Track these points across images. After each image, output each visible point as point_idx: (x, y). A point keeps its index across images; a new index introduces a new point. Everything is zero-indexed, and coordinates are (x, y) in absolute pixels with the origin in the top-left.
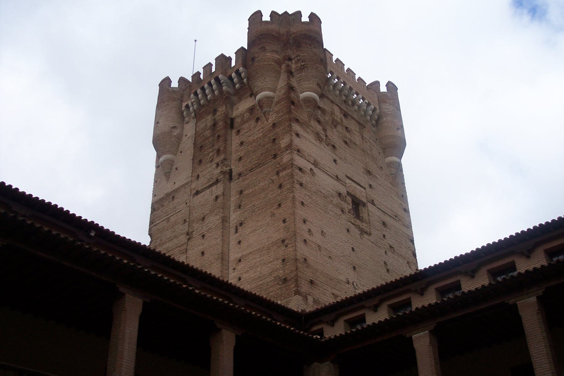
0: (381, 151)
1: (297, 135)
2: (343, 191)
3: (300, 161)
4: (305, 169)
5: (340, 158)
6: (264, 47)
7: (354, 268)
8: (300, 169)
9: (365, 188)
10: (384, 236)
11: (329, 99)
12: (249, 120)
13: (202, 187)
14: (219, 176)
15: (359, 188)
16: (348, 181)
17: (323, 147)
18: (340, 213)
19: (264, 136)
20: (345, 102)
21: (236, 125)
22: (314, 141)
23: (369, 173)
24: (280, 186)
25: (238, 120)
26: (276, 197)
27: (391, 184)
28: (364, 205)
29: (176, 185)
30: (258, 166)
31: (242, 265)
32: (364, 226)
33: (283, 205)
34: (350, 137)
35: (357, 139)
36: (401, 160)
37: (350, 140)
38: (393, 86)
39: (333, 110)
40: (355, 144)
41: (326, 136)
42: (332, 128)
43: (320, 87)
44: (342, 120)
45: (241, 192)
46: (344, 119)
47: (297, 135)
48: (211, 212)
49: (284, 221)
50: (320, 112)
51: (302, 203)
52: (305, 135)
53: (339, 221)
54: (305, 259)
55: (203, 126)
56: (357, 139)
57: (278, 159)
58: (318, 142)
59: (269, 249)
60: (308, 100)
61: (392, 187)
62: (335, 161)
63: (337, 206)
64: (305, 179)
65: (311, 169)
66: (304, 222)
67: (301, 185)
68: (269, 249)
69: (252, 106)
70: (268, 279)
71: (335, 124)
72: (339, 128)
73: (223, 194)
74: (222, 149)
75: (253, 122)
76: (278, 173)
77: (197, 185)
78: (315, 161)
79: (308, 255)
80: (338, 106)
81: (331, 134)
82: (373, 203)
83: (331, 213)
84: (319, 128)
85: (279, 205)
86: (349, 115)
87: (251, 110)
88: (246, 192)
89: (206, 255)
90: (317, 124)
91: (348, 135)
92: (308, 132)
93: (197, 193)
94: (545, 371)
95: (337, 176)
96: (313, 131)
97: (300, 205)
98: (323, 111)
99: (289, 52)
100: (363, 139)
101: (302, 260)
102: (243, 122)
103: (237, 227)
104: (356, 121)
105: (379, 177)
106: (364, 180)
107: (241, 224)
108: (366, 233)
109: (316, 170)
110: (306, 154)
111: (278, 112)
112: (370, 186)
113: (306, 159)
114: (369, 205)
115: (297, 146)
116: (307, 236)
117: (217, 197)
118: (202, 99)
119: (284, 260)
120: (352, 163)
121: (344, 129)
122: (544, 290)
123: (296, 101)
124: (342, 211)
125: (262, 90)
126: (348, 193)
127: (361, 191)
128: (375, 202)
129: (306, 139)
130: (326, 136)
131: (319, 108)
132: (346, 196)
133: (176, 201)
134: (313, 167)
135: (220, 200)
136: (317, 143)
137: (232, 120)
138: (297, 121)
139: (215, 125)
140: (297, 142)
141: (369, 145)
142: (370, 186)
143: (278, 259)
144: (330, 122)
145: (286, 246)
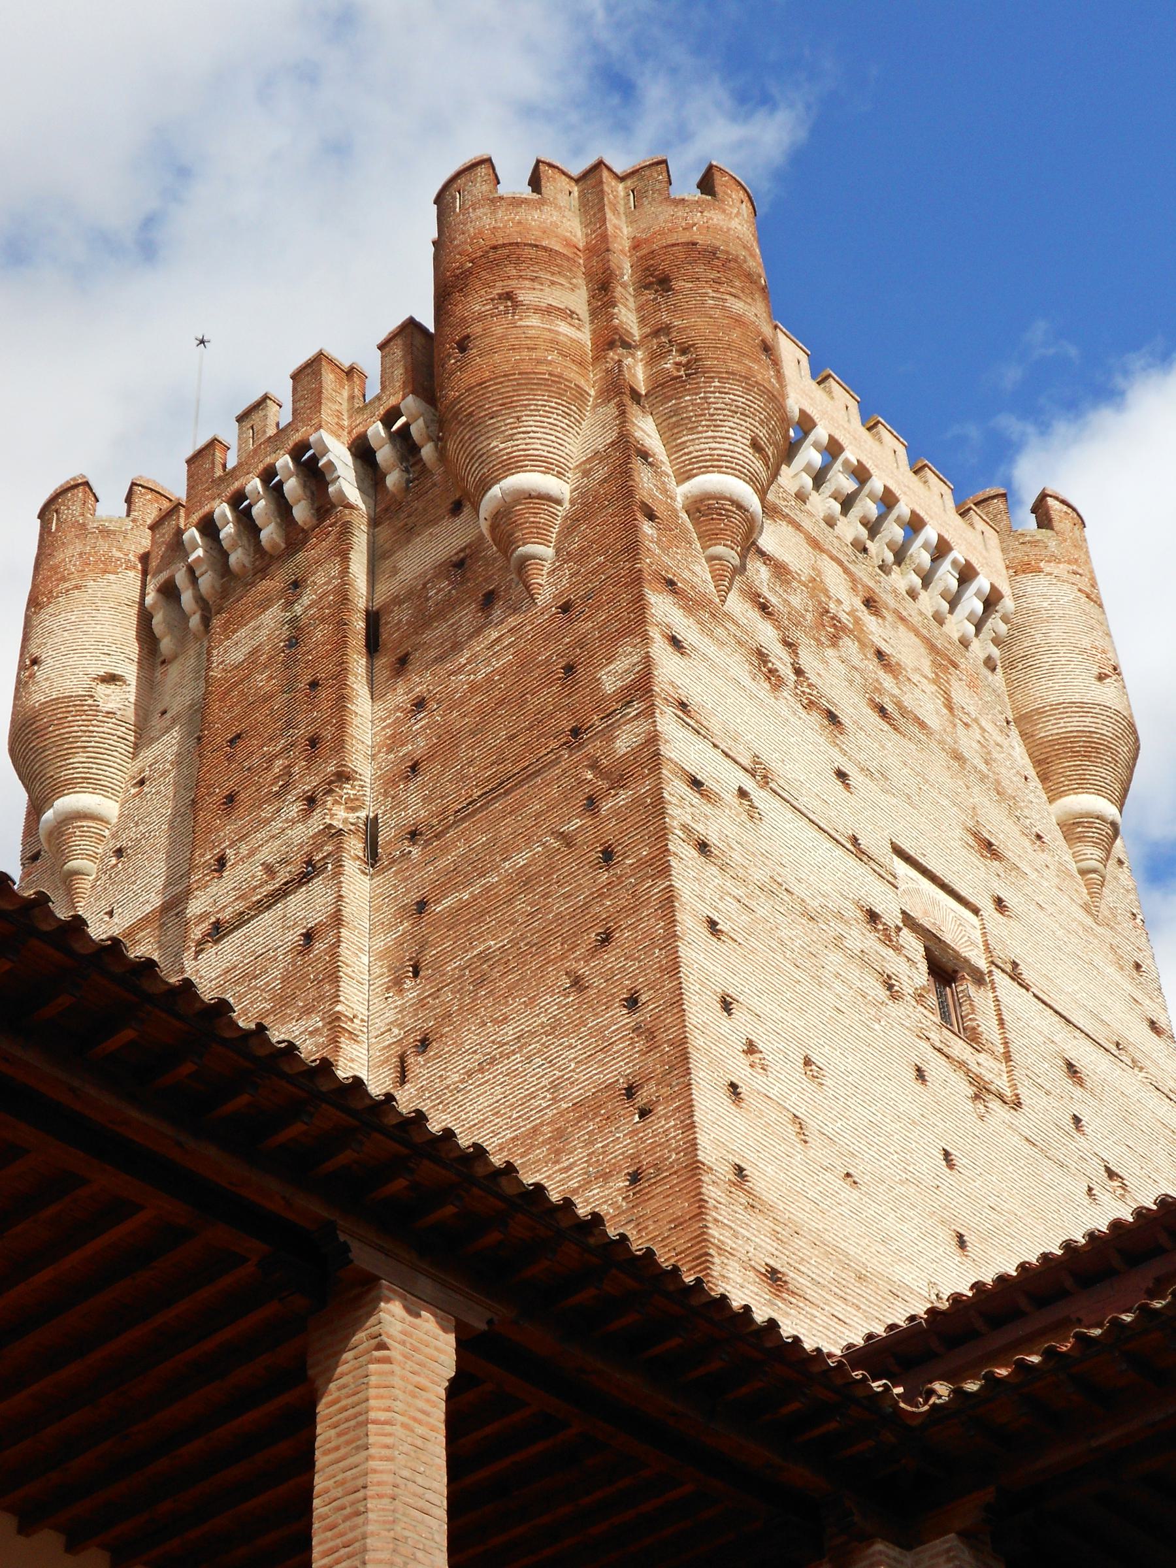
0: (1031, 772)
4: (716, 787)
5: (866, 771)
6: (509, 296)
7: (962, 1242)
8: (696, 783)
9: (976, 911)
10: (1077, 1120)
11: (798, 527)
12: (447, 607)
13: (240, 906)
14: (319, 848)
17: (785, 712)
18: (883, 993)
23: (988, 848)
24: (608, 855)
25: (402, 615)
26: (587, 905)
27: (1086, 908)
28: (979, 979)
29: (116, 919)
30: (499, 789)
32: (989, 1067)
33: (623, 936)
34: (896, 691)
35: (927, 706)
37: (899, 705)
38: (1065, 508)
39: (819, 574)
40: (922, 725)
41: (799, 672)
42: (819, 643)
44: (857, 621)
45: (421, 906)
49: (632, 1003)
53: (877, 1026)
54: (740, 1170)
55: (237, 656)
57: (589, 749)
58: (766, 685)
59: (560, 1134)
61: (1089, 921)
62: (841, 775)
65: (742, 793)
67: (703, 847)
68: (560, 1134)
69: (462, 550)
72: (849, 645)
74: (328, 733)
75: (467, 615)
76: (591, 803)
79: (752, 1156)
80: (840, 563)
82: (1015, 975)
83: (838, 987)
84: (767, 634)
85: (606, 939)
87: (460, 565)
88: (447, 903)
90: (754, 615)
91: (887, 681)
95: (855, 840)
97: (704, 931)
100: (950, 708)
101: (725, 1172)
102: (423, 621)
103: (402, 1059)
104: (917, 634)
105: (1034, 876)
107: (424, 1044)
108: (1001, 1097)
109: (759, 796)
110: (715, 725)
112: (999, 903)
113: (715, 746)
116: (739, 1069)
118: (234, 546)
119: (635, 1178)
120: (915, 798)
121: (871, 654)
123: (659, 509)
125: (512, 466)
128: (1027, 975)
130: (799, 672)
132: (899, 929)
134: (749, 785)
135: (319, 947)
141: (979, 737)
142: (999, 903)
143: (605, 1176)
144: (809, 616)
145: (644, 1113)
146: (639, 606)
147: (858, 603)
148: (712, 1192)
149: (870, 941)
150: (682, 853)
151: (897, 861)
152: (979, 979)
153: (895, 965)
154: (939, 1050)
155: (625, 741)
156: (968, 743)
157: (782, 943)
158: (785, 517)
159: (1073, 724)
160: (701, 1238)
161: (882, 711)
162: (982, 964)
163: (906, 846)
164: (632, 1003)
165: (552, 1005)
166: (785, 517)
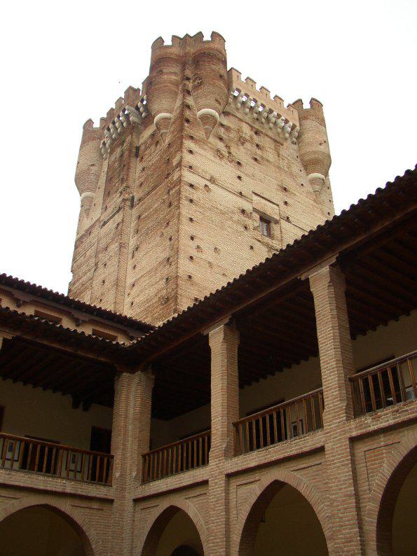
1: (191, 152)
2: (248, 207)
3: (188, 177)
5: (247, 175)
8: (191, 186)
9: (278, 205)
12: (151, 145)
15: (271, 204)
16: (255, 198)
18: (243, 229)
19: (161, 157)
20: (257, 119)
21: (141, 152)
22: (214, 159)
24: (170, 205)
25: (143, 147)
28: (277, 222)
31: (135, 289)
34: (261, 154)
36: (326, 174)
37: (262, 157)
40: (268, 161)
41: (230, 153)
43: (220, 103)
44: (251, 137)
46: (255, 136)
47: (191, 152)
48: (113, 240)
49: (170, 239)
50: (223, 130)
51: (191, 220)
52: (202, 152)
54: (190, 277)
56: (271, 156)
60: (206, 118)
62: (239, 178)
63: (238, 222)
64: (196, 195)
65: (206, 186)
66: (192, 238)
67: (191, 201)
70: (154, 301)
71: (242, 141)
72: (248, 145)
73: (123, 221)
76: (168, 193)
77: (104, 217)
78: (212, 177)
81: (237, 151)
84: (221, 145)
85: (168, 224)
86: (262, 133)
89: (106, 283)
91: (259, 152)
92: (205, 150)
93: (105, 223)
94: (330, 360)
96: (211, 148)
98: (228, 129)
99: (188, 73)
101: (186, 277)
102: (146, 149)
104: (271, 138)
106: (278, 197)
107: (137, 249)
109: (211, 186)
110: (200, 171)
111: (173, 132)
114: (283, 223)
115: (188, 162)
116: (194, 253)
117: (118, 225)
119: (167, 279)
122: (337, 255)
123: (191, 119)
124: (246, 228)
126: (255, 210)
127: (273, 209)
129: (202, 155)
130: (230, 153)
131: (222, 125)
132: (251, 213)
133: (92, 235)
134: (208, 183)
136: (217, 160)
137: (138, 148)
138: (192, 138)
139: (122, 156)
140: (188, 158)
143: (162, 279)
146: (182, 143)
147: (253, 133)
148: (180, 282)
149: (242, 217)
150: (184, 202)
151: (253, 195)
152: (277, 222)
153: (249, 222)
154: (259, 241)
155: (176, 176)
156: (283, 164)
157: (212, 221)
158: (233, 115)
159: (312, 156)
160: (176, 293)
161: (256, 160)
162: (278, 218)
163: (257, 192)
164: (170, 239)
165: (158, 239)
166: (233, 115)
